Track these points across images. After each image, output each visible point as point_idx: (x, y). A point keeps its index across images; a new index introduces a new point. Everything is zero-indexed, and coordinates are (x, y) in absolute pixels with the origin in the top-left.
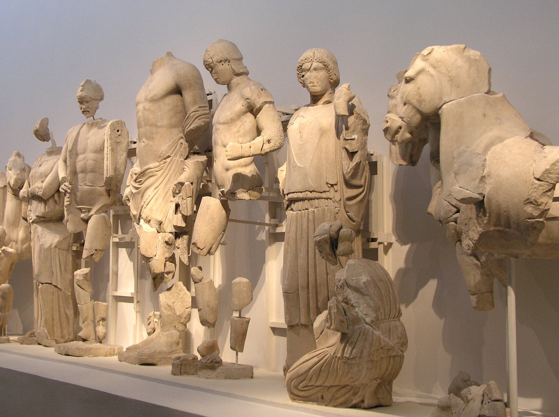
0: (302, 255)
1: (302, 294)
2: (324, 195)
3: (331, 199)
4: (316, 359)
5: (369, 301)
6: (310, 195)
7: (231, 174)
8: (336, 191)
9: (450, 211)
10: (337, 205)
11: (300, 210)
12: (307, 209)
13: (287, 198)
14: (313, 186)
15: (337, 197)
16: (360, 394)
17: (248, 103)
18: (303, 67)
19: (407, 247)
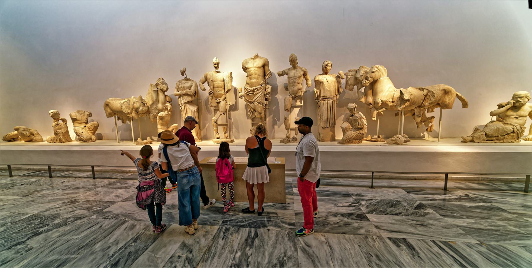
1: (329, 120)
14: (333, 94)
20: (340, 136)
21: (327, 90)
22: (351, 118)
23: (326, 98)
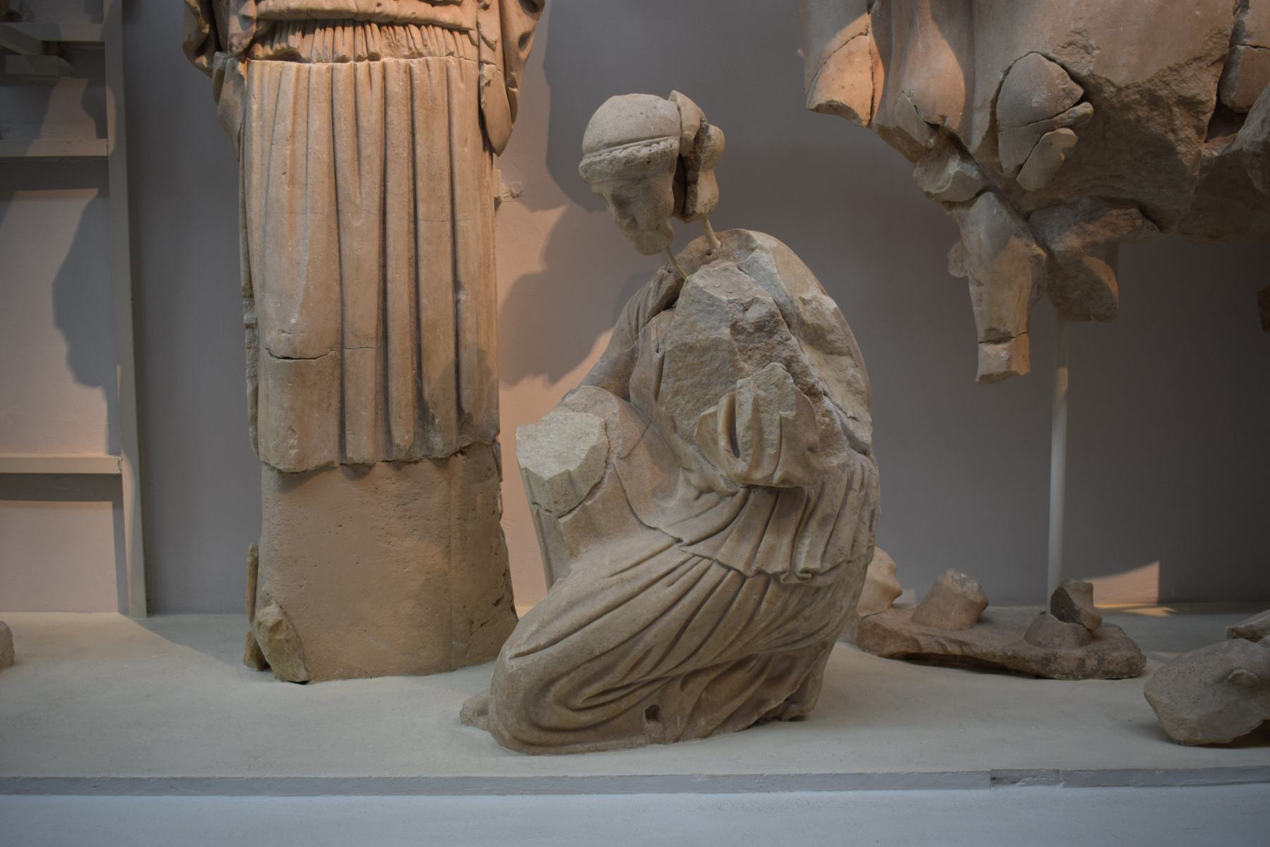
0: (362, 223)
3: (464, 31)
4: (662, 593)
5: (851, 371)
8: (486, 7)
9: (1068, 93)
10: (486, 54)
11: (343, 60)
12: (374, 57)
15: (491, 30)
16: (794, 675)
19: (553, 216)
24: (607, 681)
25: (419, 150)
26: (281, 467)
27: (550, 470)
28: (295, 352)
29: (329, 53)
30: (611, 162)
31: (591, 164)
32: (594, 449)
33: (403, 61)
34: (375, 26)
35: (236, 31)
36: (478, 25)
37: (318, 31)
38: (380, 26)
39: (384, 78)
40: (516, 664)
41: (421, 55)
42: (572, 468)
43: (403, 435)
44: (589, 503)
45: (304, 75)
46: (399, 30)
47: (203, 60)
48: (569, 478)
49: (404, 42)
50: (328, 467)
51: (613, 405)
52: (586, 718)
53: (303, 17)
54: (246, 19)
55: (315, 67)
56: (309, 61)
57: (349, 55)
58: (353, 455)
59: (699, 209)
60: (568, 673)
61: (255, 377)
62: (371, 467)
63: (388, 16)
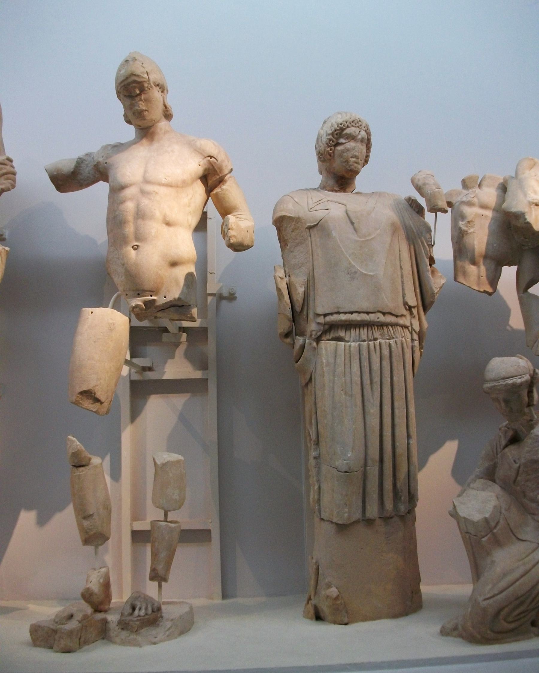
0: (373, 410)
1: (373, 471)
2: (401, 321)
3: (407, 327)
6: (382, 318)
7: (181, 273)
11: (364, 341)
12: (375, 339)
13: (321, 320)
17: (210, 163)
18: (348, 131)
20: (446, 581)
21: (353, 274)
22: (512, 452)
23: (348, 326)
24: (521, 609)
25: (395, 378)
26: (339, 522)
27: (477, 517)
28: (350, 469)
29: (358, 338)
30: (505, 385)
31: (495, 386)
32: (495, 507)
33: (387, 341)
34: (376, 327)
35: (313, 327)
36: (411, 324)
37: (352, 330)
38: (377, 326)
39: (380, 348)
40: (485, 603)
41: (393, 338)
42: (487, 516)
43: (389, 505)
44: (495, 531)
45: (347, 348)
46: (385, 328)
47: (288, 340)
48: (486, 520)
49: (386, 333)
50: (356, 522)
51: (497, 488)
52: (513, 626)
53: (347, 323)
54: (319, 324)
55: (353, 344)
56: (348, 342)
57: (366, 339)
58: (369, 515)
59: (535, 403)
60: (507, 606)
61: (318, 481)
62: (374, 520)
63: (381, 322)
